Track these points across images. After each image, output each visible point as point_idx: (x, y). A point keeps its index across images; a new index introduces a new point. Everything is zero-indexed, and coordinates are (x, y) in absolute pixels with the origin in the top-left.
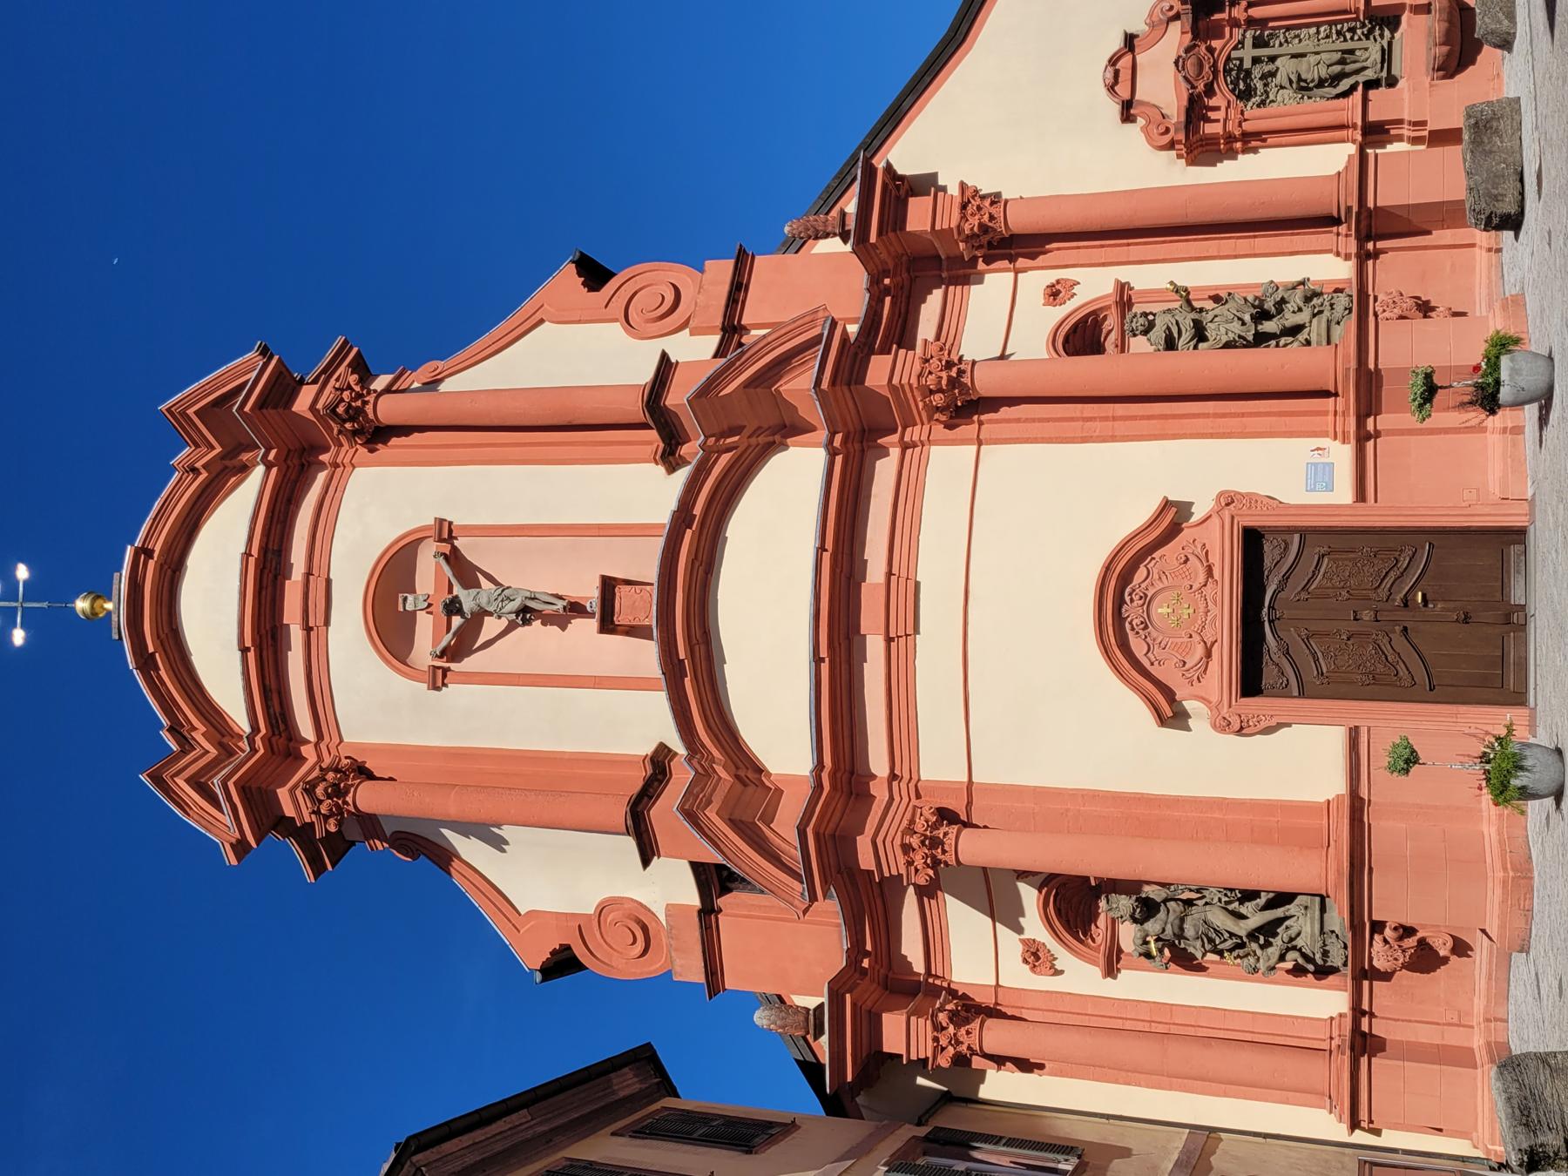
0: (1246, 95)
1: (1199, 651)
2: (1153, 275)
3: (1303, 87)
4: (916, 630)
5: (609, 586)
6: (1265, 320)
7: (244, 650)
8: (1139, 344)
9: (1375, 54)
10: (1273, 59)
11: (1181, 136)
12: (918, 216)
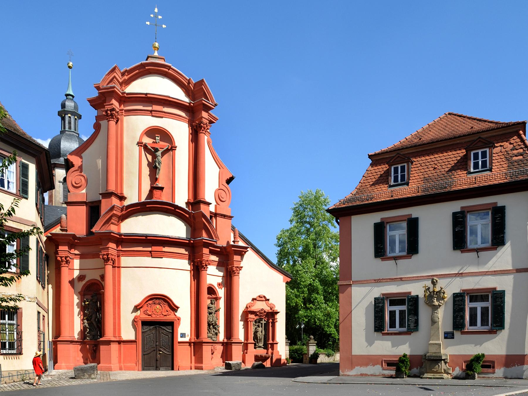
0: (256, 322)
1: (150, 314)
2: (222, 304)
3: (256, 332)
4: (153, 257)
5: (162, 189)
6: (213, 325)
7: (146, 94)
8: (209, 301)
9: (260, 345)
10: (262, 327)
11: (249, 310)
12: (236, 258)
